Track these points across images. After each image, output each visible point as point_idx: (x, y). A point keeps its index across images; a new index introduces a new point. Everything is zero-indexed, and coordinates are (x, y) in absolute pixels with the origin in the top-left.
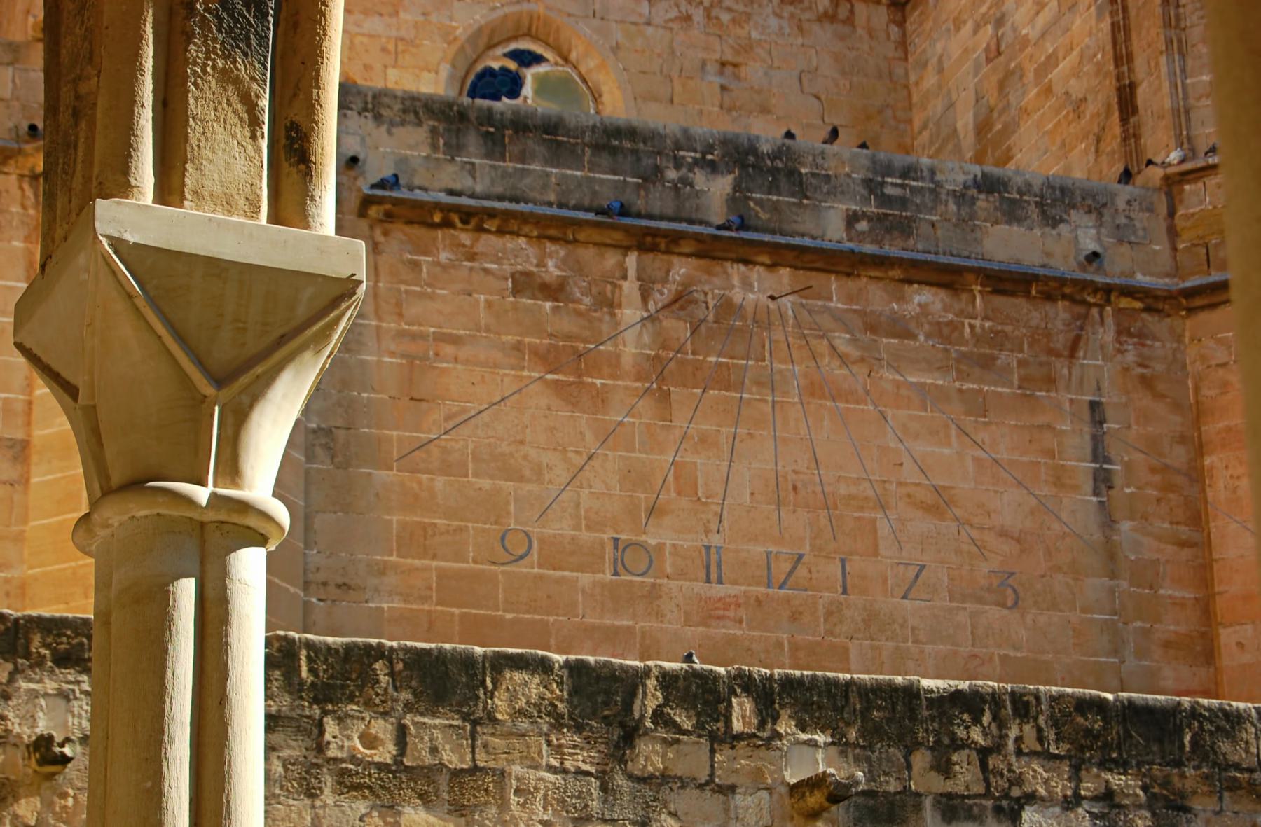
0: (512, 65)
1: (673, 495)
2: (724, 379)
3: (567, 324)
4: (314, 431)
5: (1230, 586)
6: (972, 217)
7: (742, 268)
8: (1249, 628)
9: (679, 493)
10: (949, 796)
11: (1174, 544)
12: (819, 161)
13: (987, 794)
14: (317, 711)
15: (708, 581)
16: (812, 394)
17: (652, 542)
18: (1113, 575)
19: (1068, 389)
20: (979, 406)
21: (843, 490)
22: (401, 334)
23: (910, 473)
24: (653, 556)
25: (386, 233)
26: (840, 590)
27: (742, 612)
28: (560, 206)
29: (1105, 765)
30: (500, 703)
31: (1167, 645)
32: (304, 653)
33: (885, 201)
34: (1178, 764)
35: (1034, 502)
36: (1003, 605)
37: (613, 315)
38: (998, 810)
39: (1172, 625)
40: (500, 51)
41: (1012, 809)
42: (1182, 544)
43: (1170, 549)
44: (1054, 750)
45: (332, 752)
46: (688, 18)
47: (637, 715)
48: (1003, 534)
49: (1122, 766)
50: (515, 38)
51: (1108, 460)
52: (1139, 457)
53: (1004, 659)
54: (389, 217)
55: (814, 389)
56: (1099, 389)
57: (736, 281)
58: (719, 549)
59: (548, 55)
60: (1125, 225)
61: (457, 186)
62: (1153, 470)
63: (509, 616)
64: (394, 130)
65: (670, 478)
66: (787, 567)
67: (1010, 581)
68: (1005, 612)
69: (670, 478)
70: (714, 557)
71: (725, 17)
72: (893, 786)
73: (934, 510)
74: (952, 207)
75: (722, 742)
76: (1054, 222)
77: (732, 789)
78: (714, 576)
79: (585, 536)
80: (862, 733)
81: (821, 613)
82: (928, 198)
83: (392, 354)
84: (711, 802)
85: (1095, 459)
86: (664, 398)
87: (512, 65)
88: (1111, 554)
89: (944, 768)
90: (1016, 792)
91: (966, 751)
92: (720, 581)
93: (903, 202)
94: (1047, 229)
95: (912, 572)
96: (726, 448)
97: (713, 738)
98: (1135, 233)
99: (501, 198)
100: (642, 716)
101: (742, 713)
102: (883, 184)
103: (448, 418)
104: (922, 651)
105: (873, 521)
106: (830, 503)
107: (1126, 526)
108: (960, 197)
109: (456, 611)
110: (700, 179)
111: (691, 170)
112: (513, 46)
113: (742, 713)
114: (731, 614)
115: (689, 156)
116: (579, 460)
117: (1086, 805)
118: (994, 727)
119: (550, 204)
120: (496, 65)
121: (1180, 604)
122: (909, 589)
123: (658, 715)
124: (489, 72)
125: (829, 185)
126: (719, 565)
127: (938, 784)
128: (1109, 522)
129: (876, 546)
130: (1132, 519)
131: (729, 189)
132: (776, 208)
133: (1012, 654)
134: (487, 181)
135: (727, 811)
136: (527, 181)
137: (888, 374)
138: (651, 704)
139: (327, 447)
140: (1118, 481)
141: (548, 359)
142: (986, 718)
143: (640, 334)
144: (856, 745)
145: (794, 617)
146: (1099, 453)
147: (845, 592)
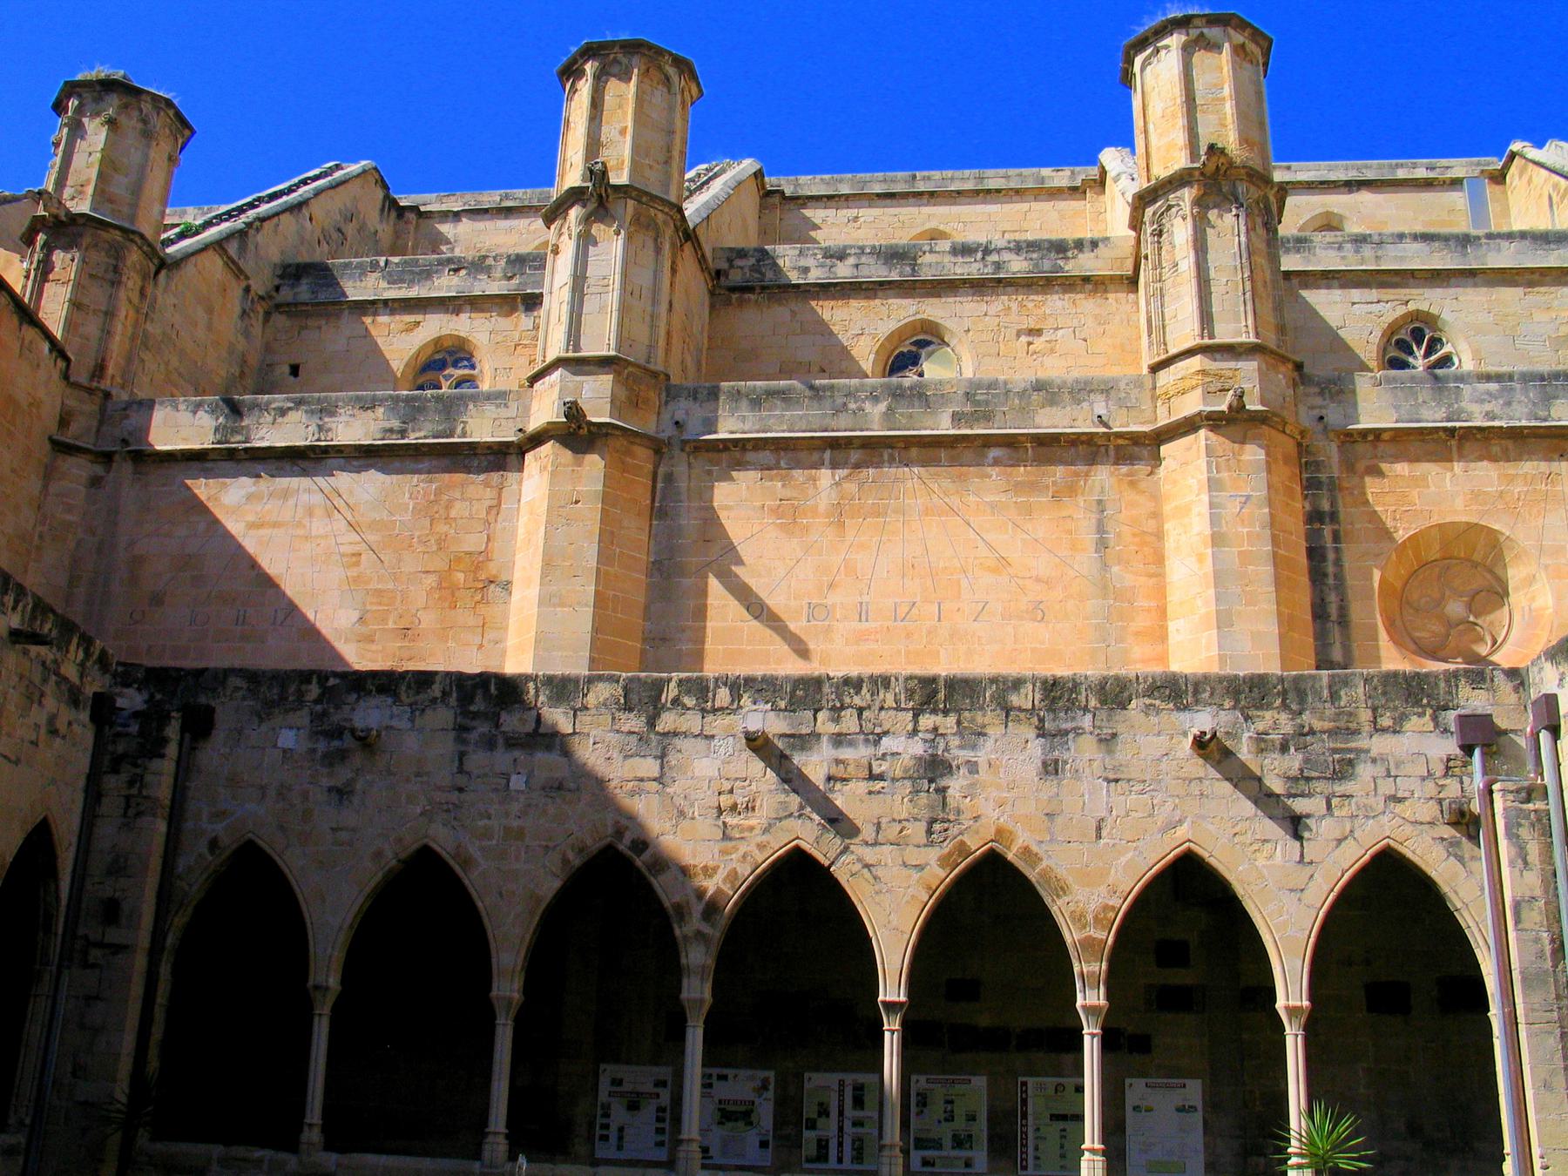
0: (914, 349)
1: (843, 577)
2: (877, 512)
3: (788, 493)
4: (653, 563)
5: (1174, 597)
6: (1029, 404)
7: (890, 450)
8: (1182, 620)
9: (846, 576)
10: (839, 734)
11: (1146, 576)
12: (938, 386)
13: (861, 731)
14: (498, 709)
15: (860, 620)
16: (927, 515)
17: (829, 602)
18: (1105, 597)
19: (1083, 494)
20: (1028, 511)
21: (941, 565)
22: (702, 508)
23: (983, 551)
24: (829, 611)
25: (695, 458)
26: (936, 619)
27: (878, 636)
28: (790, 431)
29: (934, 711)
30: (591, 700)
31: (1137, 633)
32: (493, 680)
33: (978, 403)
34: (982, 708)
35: (1057, 560)
36: (1034, 620)
37: (815, 485)
38: (867, 741)
39: (1141, 622)
40: (908, 342)
41: (875, 740)
42: (1151, 576)
43: (1143, 579)
44: (903, 706)
45: (503, 729)
46: (1009, 308)
47: (663, 700)
48: (1038, 580)
49: (946, 712)
50: (912, 336)
51: (1107, 533)
52: (1125, 528)
53: (1033, 650)
54: (696, 448)
55: (927, 511)
56: (1102, 492)
57: (886, 457)
58: (867, 603)
59: (934, 340)
60: (1125, 398)
61: (734, 429)
62: (1134, 535)
63: (749, 648)
64: (704, 405)
65: (842, 568)
66: (907, 609)
67: (1041, 606)
68: (1036, 624)
69: (842, 568)
70: (864, 607)
71: (1030, 305)
72: (805, 730)
73: (995, 571)
74: (1017, 401)
75: (708, 712)
76: (1079, 402)
77: (713, 737)
78: (863, 618)
79: (793, 603)
80: (791, 703)
81: (924, 634)
82: (1002, 398)
83: (696, 519)
84: (701, 743)
85: (1098, 532)
86: (842, 525)
87: (914, 349)
88: (1104, 587)
89: (837, 720)
90: (878, 730)
91: (850, 709)
92: (867, 621)
93: (987, 403)
94: (1074, 407)
95: (980, 606)
96: (875, 549)
97: (703, 711)
98: (1130, 401)
99: (758, 432)
100: (666, 701)
101: (723, 696)
102: (975, 395)
103: (722, 549)
104: (983, 649)
105: (959, 581)
106: (934, 573)
107: (1115, 569)
108: (1022, 394)
109: (720, 647)
110: (868, 406)
111: (864, 402)
112: (915, 339)
113: (723, 696)
114: (873, 637)
115: (863, 395)
116: (792, 564)
117: (920, 735)
118: (868, 696)
119: (783, 431)
120: (905, 350)
121: (1149, 611)
122: (977, 617)
123: (676, 701)
124: (902, 354)
125: (944, 399)
126: (867, 612)
127: (833, 728)
128: (1105, 566)
129: (960, 594)
130: (1119, 564)
131: (884, 410)
132: (911, 416)
133: (1038, 646)
134: (750, 424)
135: (709, 748)
136: (772, 421)
137: (972, 498)
138: (671, 695)
139: (659, 570)
140: (1111, 544)
141: (776, 512)
142: (864, 690)
143: (830, 493)
144: (786, 710)
145: (908, 636)
146: (1101, 529)
147: (939, 620)
